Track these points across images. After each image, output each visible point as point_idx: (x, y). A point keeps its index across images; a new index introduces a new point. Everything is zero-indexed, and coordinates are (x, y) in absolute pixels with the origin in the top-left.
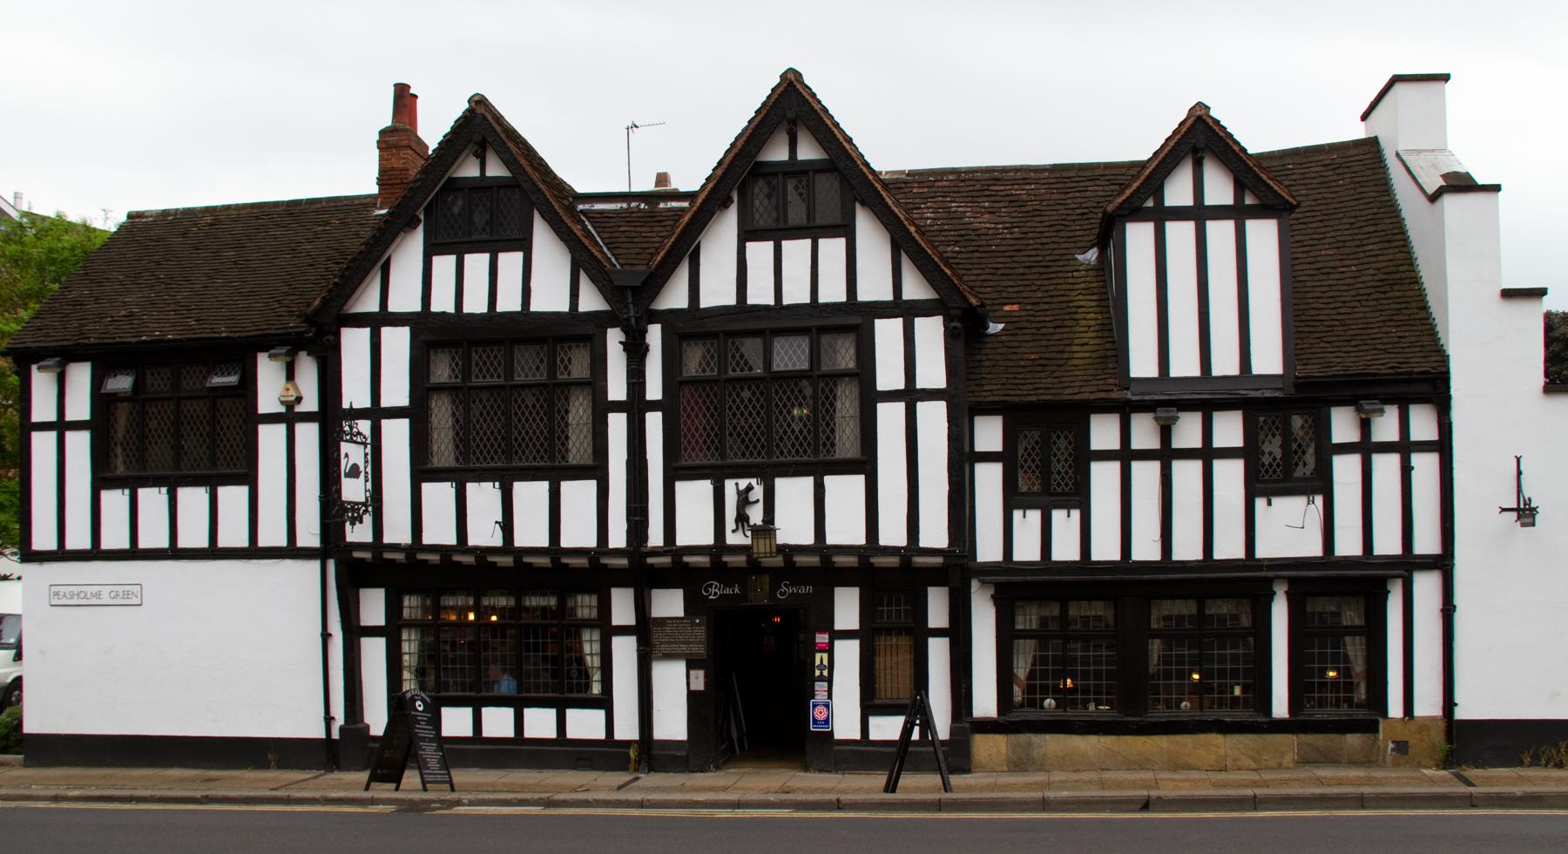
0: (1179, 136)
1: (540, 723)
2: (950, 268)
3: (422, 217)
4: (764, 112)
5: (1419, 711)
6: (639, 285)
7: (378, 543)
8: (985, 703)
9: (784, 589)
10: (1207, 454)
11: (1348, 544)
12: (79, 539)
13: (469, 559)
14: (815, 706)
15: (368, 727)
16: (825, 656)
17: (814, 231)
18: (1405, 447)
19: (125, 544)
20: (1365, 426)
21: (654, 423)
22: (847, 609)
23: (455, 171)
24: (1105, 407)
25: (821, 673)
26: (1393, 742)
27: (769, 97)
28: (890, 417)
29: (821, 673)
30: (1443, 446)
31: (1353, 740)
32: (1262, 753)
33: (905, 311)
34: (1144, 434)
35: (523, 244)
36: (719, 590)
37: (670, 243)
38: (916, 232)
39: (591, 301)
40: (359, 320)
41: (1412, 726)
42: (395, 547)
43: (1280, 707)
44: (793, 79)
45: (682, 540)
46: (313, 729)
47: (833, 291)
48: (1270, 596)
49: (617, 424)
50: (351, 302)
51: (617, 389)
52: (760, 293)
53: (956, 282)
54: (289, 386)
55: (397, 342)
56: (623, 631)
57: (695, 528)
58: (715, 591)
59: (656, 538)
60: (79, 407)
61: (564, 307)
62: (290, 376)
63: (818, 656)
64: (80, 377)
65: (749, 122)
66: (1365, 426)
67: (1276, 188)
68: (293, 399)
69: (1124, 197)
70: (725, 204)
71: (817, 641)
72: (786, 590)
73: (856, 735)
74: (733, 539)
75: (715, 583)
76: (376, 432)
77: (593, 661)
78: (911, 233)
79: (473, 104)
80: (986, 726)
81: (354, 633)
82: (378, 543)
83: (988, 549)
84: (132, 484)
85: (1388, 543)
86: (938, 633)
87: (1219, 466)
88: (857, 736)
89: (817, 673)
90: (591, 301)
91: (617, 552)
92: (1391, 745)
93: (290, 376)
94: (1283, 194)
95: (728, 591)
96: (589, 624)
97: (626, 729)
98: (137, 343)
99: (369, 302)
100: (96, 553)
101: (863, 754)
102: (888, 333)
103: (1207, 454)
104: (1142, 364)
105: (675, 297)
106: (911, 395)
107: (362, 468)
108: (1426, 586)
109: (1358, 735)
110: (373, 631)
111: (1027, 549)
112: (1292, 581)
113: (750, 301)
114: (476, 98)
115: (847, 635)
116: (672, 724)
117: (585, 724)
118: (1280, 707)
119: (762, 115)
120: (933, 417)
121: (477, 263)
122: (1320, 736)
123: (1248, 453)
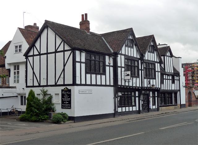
12: (83, 82)
28: (157, 73)
30: (179, 80)
33: (157, 62)
39: (138, 57)
45: (145, 86)
49: (140, 71)
51: (140, 68)
55: (123, 57)
59: (143, 86)
62: (109, 60)
64: (83, 55)
74: (148, 86)
84: (91, 74)
86: (156, 97)
90: (138, 57)
97: (137, 109)
100: (86, 85)
104: (166, 71)
117: (134, 109)
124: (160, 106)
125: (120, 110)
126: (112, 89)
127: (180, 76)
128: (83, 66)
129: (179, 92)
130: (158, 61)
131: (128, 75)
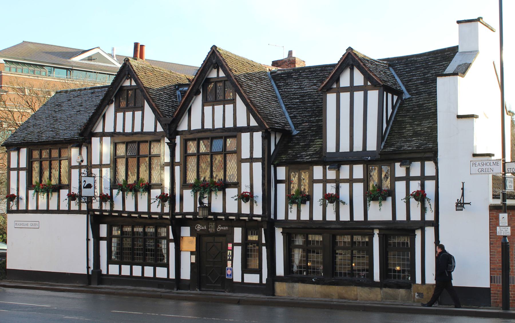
0: (342, 61)
1: (149, 272)
2: (260, 115)
3: (114, 100)
4: (206, 61)
5: (427, 282)
6: (170, 123)
7: (101, 210)
8: (280, 271)
9: (219, 228)
10: (351, 181)
11: (401, 216)
13: (126, 215)
14: (227, 269)
15: (101, 271)
16: (231, 252)
17: (224, 102)
18: (423, 178)
19: (56, 208)
20: (408, 171)
21: (177, 169)
22: (238, 233)
23: (123, 83)
24: (317, 163)
25: (229, 258)
26: (417, 293)
27: (207, 56)
28: (245, 166)
29: (229, 258)
30: (436, 178)
31: (402, 292)
32: (370, 294)
33: (249, 129)
34: (331, 175)
35: (142, 109)
36: (200, 227)
37: (179, 109)
38: (250, 102)
40: (96, 135)
41: (424, 287)
42: (106, 211)
43: (377, 277)
44: (214, 49)
46: (83, 271)
47: (229, 124)
48: (373, 235)
50: (94, 129)
52: (208, 125)
53: (262, 120)
54: (79, 156)
56: (171, 241)
57: (189, 206)
58: (199, 227)
59: (177, 210)
60: (23, 164)
61: (153, 130)
62: (80, 154)
63: (229, 251)
65: (202, 65)
66: (408, 171)
67: (375, 78)
68: (80, 161)
69: (323, 85)
70: (197, 93)
71: (228, 246)
72: (220, 228)
73: (240, 280)
75: (199, 225)
76: (101, 171)
77: (164, 251)
78: (248, 103)
79: (125, 61)
80: (281, 279)
81: (97, 239)
82: (112, 211)
83: (281, 216)
85: (416, 216)
87: (355, 185)
88: (240, 281)
89: (228, 258)
90: (160, 129)
91: (167, 214)
92: (416, 294)
93: (80, 154)
94: (378, 81)
95: (203, 228)
96: (164, 238)
97: (172, 276)
98: (38, 142)
99: (99, 129)
101: (243, 286)
102: (245, 137)
103: (351, 181)
104: (331, 148)
105: (183, 127)
106: (252, 160)
107: (93, 185)
108: (430, 231)
109: (404, 290)
110: (103, 239)
111: (293, 216)
112: (380, 229)
113: (205, 128)
114: (126, 59)
115: (238, 244)
116: (186, 274)
117: (161, 273)
118: (377, 277)
119: (205, 63)
120: (258, 167)
121: (129, 114)
122: (391, 289)
123: (366, 180)
124: (281, 279)
125: (114, 270)
126: (83, 218)
127: (434, 158)
128: (23, 174)
129: (430, 231)
130: (253, 123)
131: (89, 186)
